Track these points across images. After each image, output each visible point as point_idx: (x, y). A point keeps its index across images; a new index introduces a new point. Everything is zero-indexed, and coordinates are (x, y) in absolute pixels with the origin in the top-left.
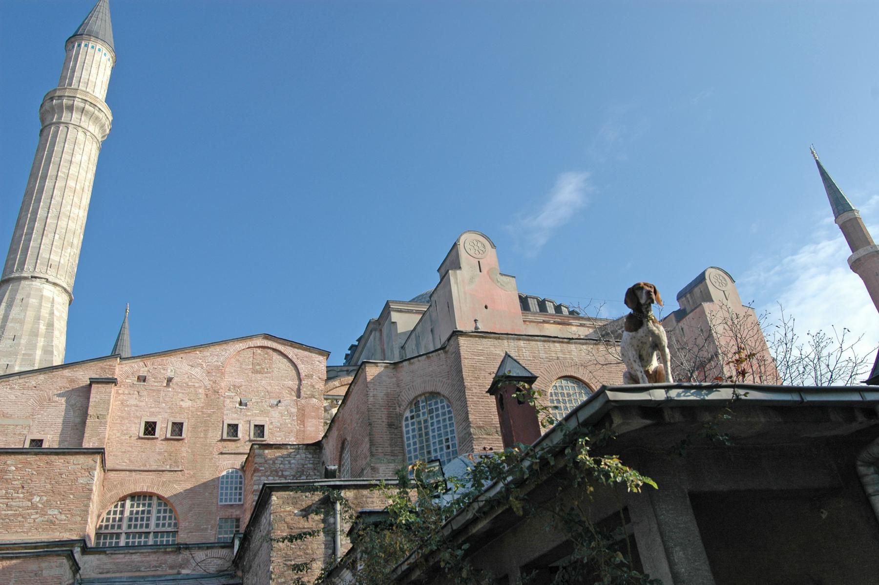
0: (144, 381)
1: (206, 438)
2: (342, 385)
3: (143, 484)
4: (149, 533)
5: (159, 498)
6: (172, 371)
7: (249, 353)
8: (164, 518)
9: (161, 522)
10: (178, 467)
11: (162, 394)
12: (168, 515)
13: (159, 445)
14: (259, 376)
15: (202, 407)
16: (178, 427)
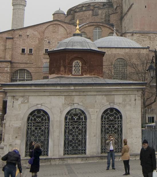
0: (21, 36)
1: (39, 53)
2: (89, 26)
3: (22, 66)
4: (25, 80)
5: (27, 70)
6: (28, 33)
7: (51, 26)
8: (28, 76)
9: (28, 77)
10: (31, 62)
11: (26, 40)
12: (29, 75)
13: (26, 56)
14: (54, 34)
15: (38, 44)
16: (31, 50)
